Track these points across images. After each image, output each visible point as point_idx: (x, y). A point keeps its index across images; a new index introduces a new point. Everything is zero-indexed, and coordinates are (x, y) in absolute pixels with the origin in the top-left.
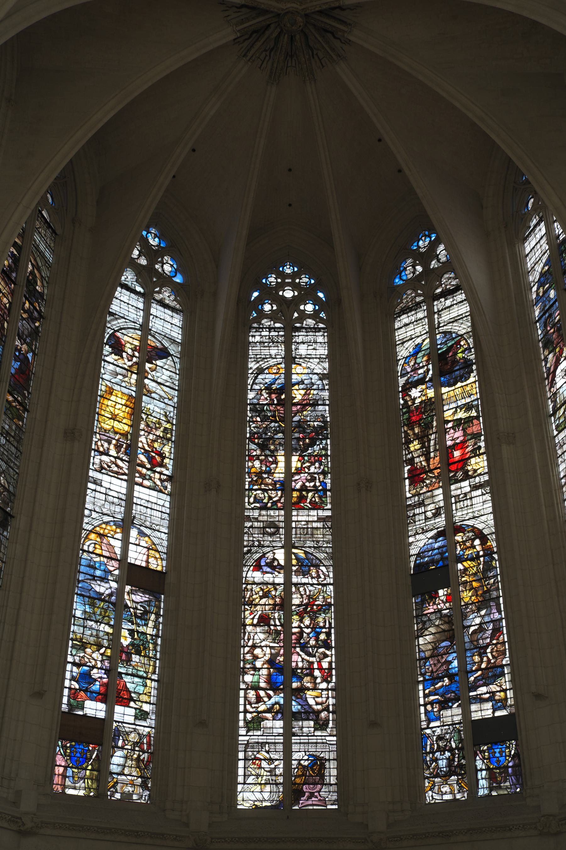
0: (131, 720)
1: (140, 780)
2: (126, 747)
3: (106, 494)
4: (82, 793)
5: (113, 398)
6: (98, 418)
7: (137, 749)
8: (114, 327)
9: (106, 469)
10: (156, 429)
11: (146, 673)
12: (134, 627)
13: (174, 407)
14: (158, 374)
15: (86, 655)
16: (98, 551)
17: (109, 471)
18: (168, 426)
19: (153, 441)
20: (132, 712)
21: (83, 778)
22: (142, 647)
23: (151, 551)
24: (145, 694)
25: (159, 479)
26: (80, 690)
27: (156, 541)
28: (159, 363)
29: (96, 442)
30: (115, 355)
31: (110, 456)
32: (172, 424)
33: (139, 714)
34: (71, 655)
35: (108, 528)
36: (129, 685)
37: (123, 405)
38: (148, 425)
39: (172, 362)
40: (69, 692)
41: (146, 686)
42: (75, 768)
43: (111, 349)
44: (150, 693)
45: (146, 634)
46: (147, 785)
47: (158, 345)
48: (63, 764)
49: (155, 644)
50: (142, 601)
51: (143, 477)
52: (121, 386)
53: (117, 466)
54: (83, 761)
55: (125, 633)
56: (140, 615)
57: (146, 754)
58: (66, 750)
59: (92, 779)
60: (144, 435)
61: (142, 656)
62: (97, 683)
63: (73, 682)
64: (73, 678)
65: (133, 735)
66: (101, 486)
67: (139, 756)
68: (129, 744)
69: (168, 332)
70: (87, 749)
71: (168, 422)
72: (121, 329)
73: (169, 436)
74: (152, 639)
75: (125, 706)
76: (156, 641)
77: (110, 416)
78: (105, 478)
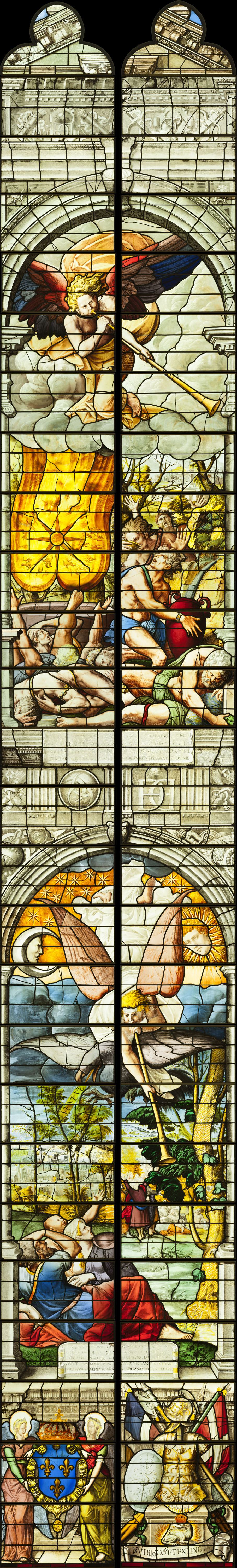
0: (172, 1370)
1: (203, 1510)
2: (161, 1438)
3: (57, 786)
4: (75, 1558)
5: (49, 482)
6: (10, 564)
7: (191, 1437)
8: (27, 240)
9: (50, 712)
10: (176, 529)
11: (201, 1245)
12: (156, 1133)
13: (225, 434)
14: (166, 343)
15: (48, 1233)
16: (53, 955)
17: (62, 714)
18: (212, 505)
19: (167, 573)
20: (171, 1351)
21: (74, 1525)
22: (183, 1180)
23: (186, 912)
24: (204, 1300)
25: (195, 688)
26: (44, 1321)
27: (200, 876)
28: (166, 301)
29: (13, 640)
30: (41, 336)
31: (58, 669)
32: (224, 493)
33: (191, 1353)
34: (12, 1241)
35: (72, 879)
36: (155, 1287)
37: (79, 493)
38: (147, 530)
39: (211, 278)
40: (17, 1330)
41: (203, 1279)
42: (52, 1504)
43: (25, 323)
44: (216, 1294)
45: (191, 1144)
46: (224, 1519)
47: (162, 237)
48: (23, 1498)
49: (220, 1164)
50: (174, 1057)
51: (146, 697)
52: (66, 433)
53: (84, 690)
54: (71, 1486)
55: (132, 1154)
56: (171, 1097)
57: (217, 1448)
58: (25, 1466)
59: (97, 1524)
60: (138, 565)
61: (187, 1204)
62: (86, 1296)
63: (23, 1307)
64: (21, 1297)
65: (177, 1406)
66: (42, 766)
67: (197, 1454)
68: (170, 1430)
69: (185, 171)
70: (76, 1456)
71: (212, 491)
72: (50, 239)
73: (216, 536)
74: (212, 1153)
75: (149, 1340)
76: (223, 1153)
77: (44, 546)
78: (53, 738)
